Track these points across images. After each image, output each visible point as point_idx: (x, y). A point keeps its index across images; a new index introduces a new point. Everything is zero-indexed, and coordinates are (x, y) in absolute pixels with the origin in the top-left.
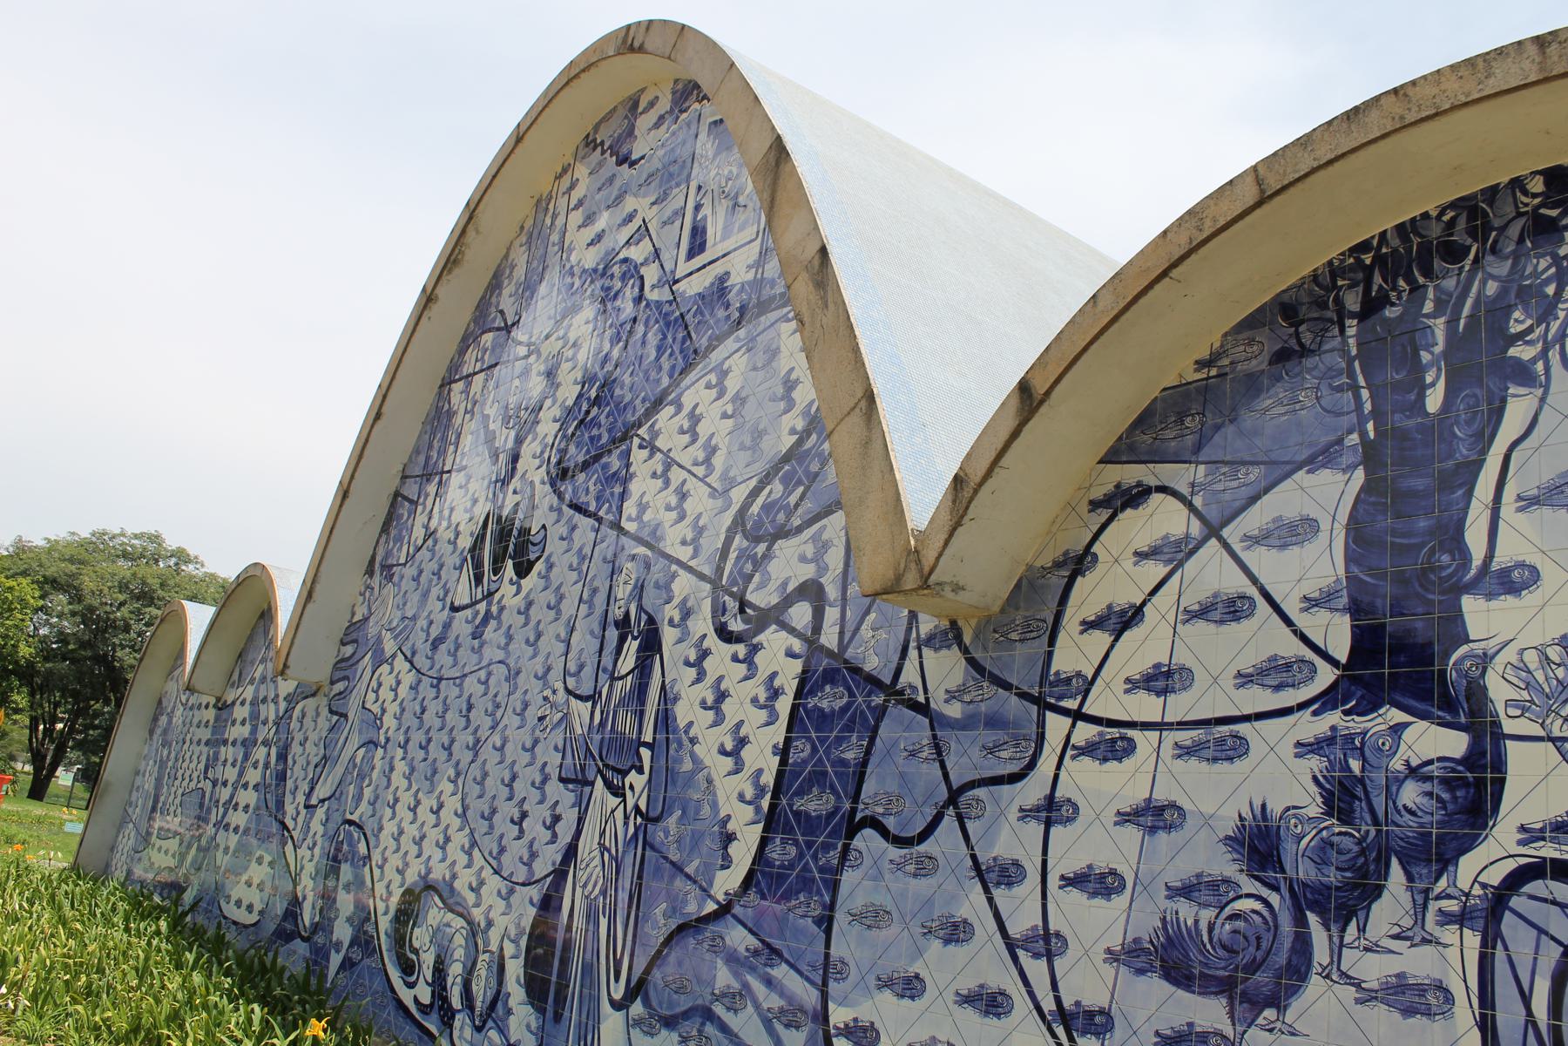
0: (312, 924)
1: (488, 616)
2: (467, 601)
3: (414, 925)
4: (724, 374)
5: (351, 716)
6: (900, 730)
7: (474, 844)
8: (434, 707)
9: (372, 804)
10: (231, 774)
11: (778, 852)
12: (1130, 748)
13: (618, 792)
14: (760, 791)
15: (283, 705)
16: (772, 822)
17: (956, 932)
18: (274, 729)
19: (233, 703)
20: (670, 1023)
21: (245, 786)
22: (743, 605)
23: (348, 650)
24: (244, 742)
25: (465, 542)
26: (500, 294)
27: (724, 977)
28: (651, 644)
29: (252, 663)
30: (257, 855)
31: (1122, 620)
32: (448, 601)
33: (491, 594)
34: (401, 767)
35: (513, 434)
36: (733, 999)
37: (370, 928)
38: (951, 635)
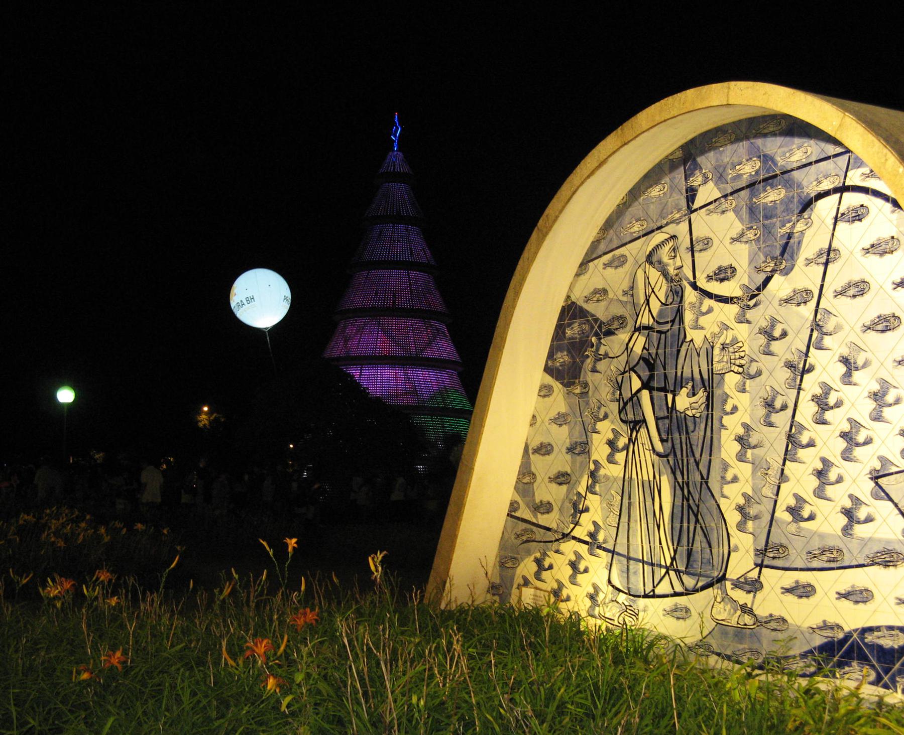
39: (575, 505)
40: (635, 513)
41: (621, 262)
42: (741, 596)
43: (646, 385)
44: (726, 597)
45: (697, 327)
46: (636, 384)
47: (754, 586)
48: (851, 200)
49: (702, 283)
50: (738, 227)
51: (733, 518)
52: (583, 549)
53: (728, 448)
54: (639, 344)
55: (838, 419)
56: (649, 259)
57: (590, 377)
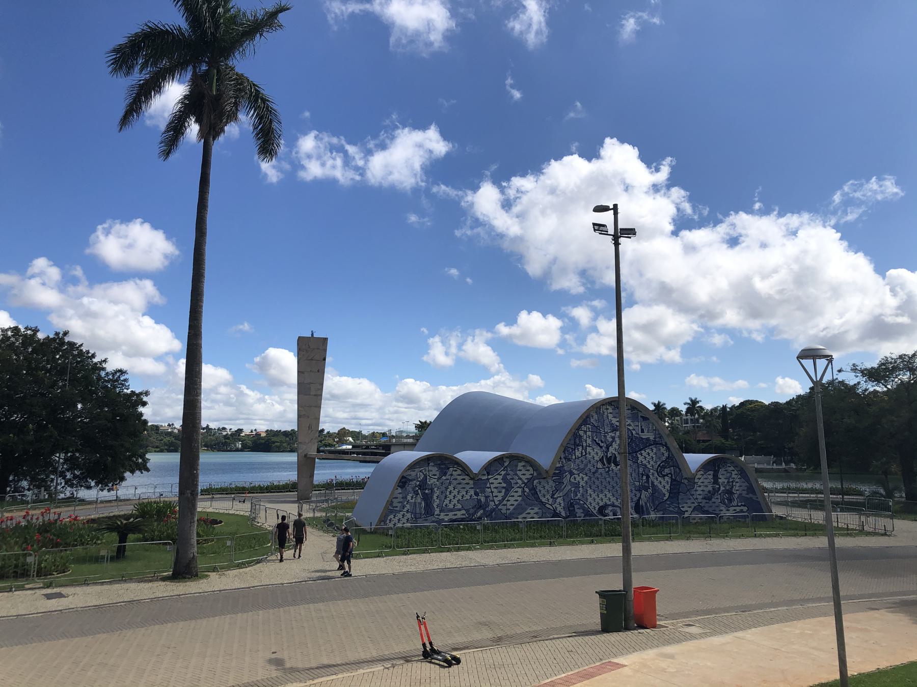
0: (566, 515)
1: (609, 470)
2: (601, 467)
3: (605, 510)
4: (652, 450)
5: (565, 483)
6: (682, 485)
7: (617, 499)
8: (597, 482)
9: (583, 495)
10: (503, 494)
11: (671, 495)
12: (700, 487)
13: (647, 491)
14: (668, 490)
15: (526, 481)
16: (670, 493)
17: (690, 499)
18: (524, 485)
19: (488, 479)
20: (661, 511)
21: (513, 496)
22: (662, 474)
23: (558, 472)
24: (503, 488)
25: (597, 458)
26: (590, 419)
27: (667, 506)
28: (648, 477)
29: (497, 471)
30: (530, 508)
31: (699, 479)
32: (595, 467)
33: (608, 468)
34: (590, 491)
35: (605, 445)
36: (668, 508)
37: (591, 513)
38: (686, 478)
39: (403, 507)
40: (417, 506)
41: (414, 471)
42: (437, 517)
43: (419, 489)
44: (434, 517)
45: (429, 481)
46: (417, 489)
47: (440, 515)
48: (454, 469)
49: (430, 476)
50: (437, 469)
51: (436, 507)
52: (405, 513)
53: (435, 498)
54: (418, 483)
55: (453, 494)
56: (420, 471)
57: (407, 488)
